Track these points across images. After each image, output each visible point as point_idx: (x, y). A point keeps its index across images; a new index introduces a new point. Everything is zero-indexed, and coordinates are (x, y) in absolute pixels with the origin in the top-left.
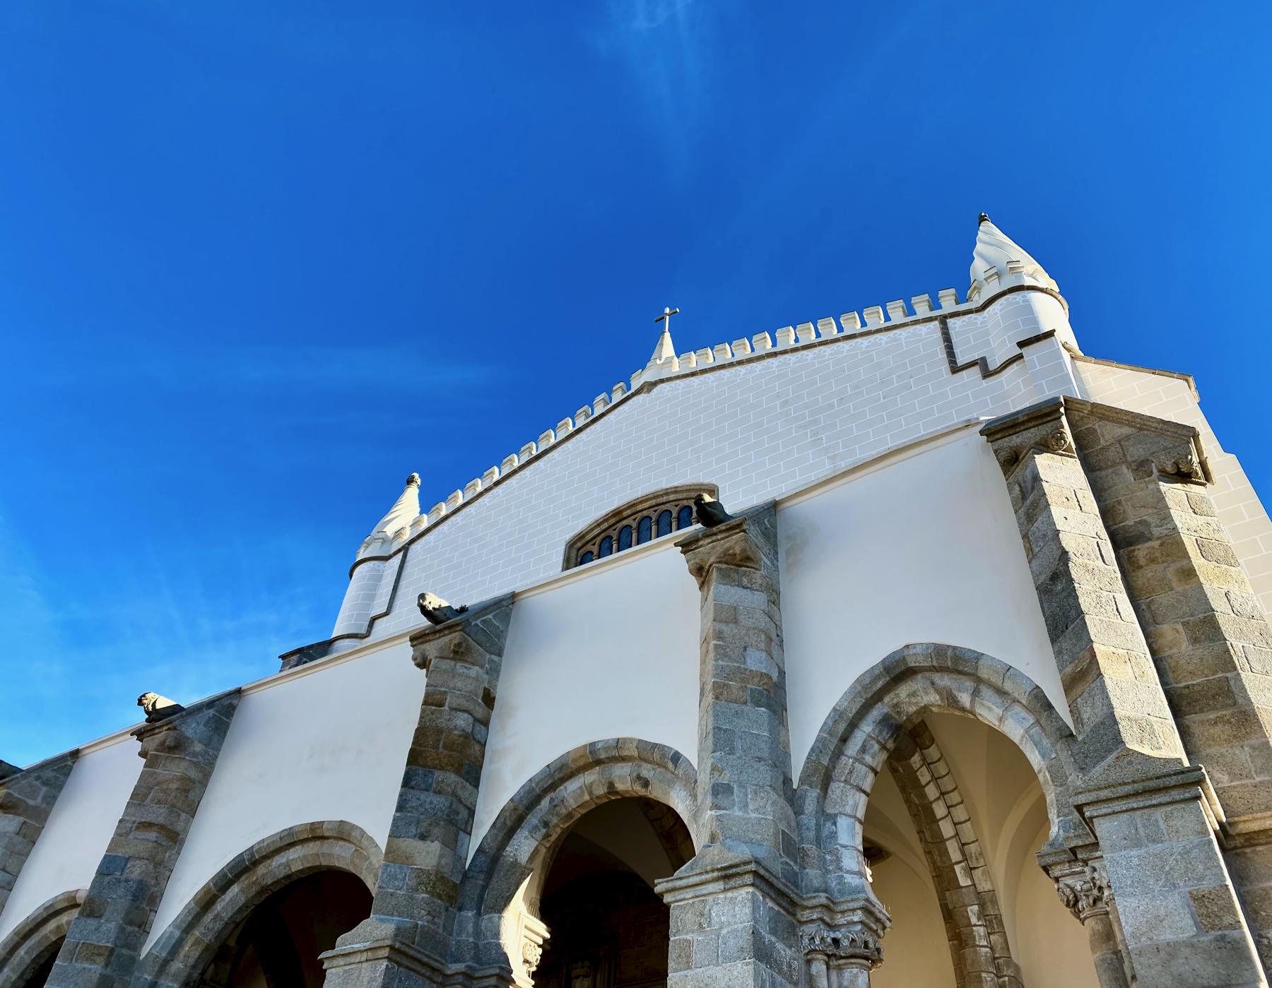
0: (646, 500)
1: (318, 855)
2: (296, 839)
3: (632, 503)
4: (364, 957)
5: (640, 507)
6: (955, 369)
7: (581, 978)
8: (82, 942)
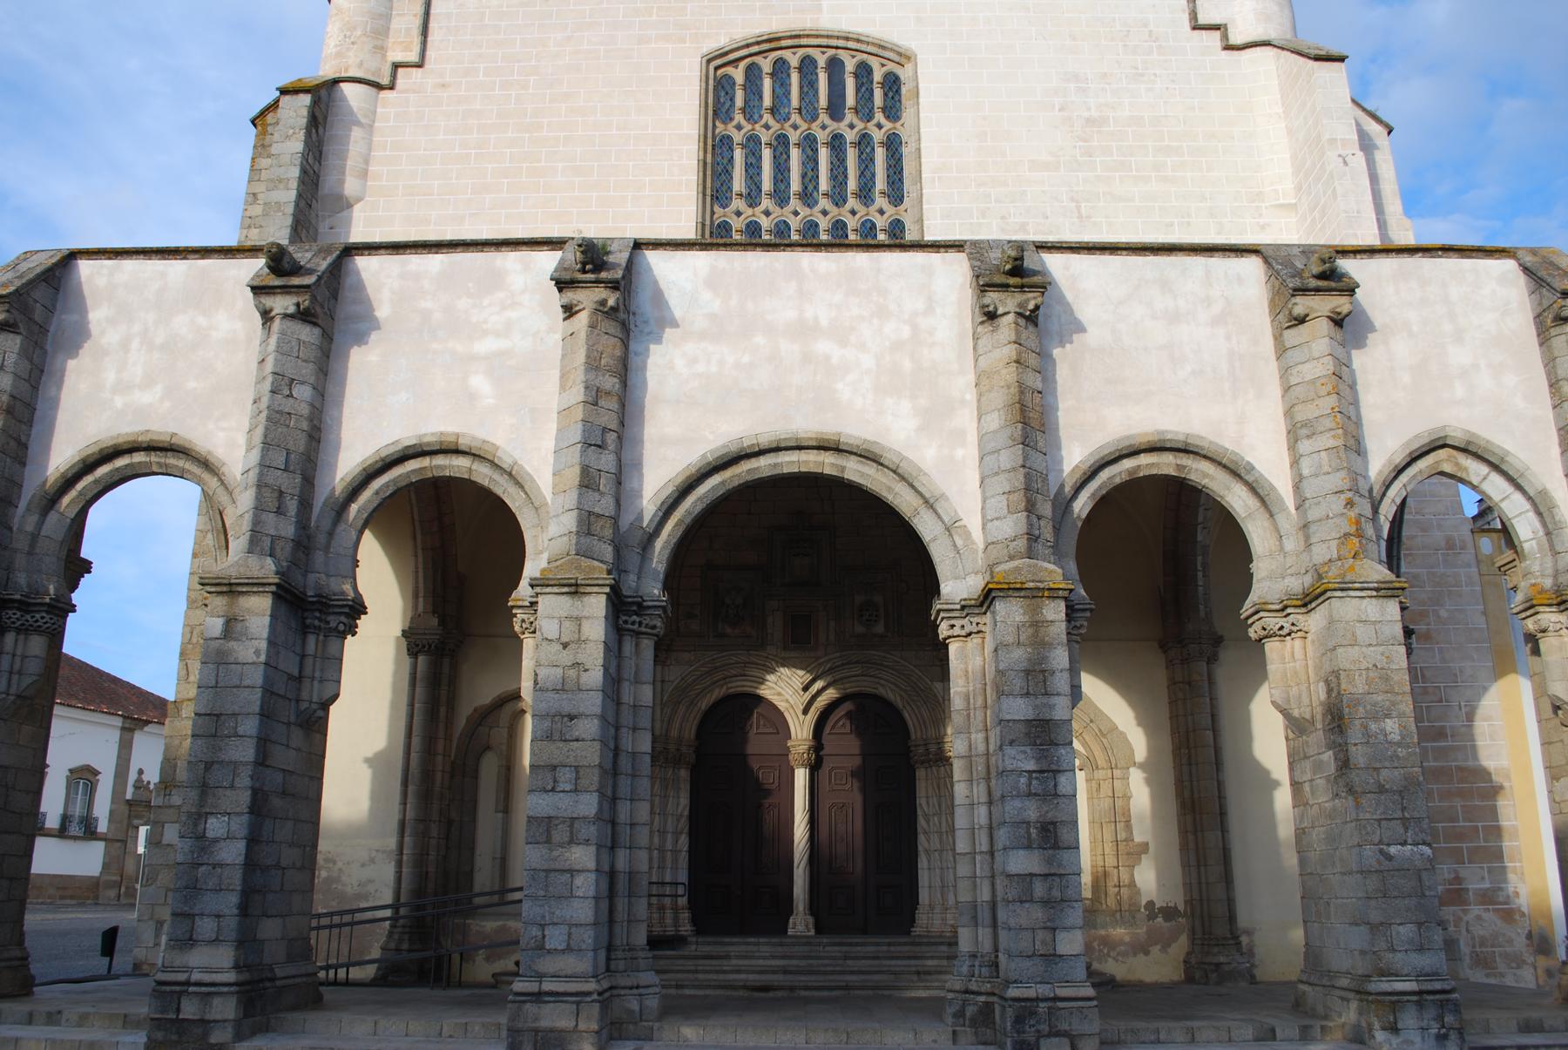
0: (817, 36)
3: (798, 33)
5: (804, 41)
6: (1197, 27)
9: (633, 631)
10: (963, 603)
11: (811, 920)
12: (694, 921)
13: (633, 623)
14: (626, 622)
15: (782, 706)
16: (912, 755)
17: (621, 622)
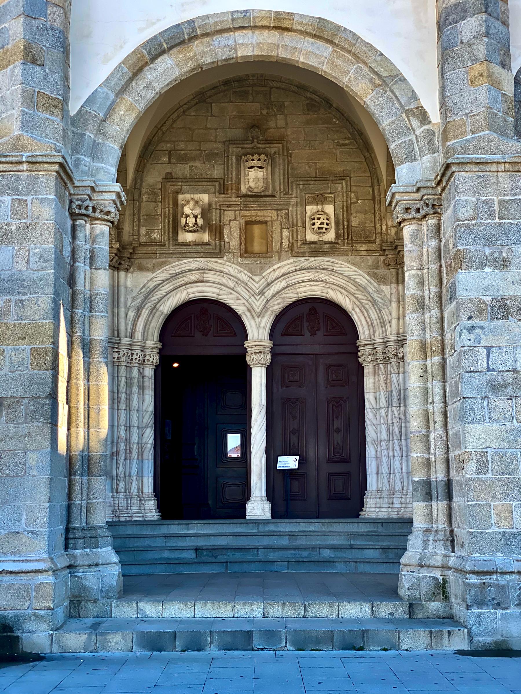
1: (278, 46)
2: (252, 24)
4: (502, 167)
7: (256, 168)
8: (37, 90)
9: (87, 216)
10: (418, 185)
11: (267, 505)
12: (161, 507)
13: (87, 208)
14: (79, 207)
15: (239, 308)
16: (360, 354)
17: (74, 206)
